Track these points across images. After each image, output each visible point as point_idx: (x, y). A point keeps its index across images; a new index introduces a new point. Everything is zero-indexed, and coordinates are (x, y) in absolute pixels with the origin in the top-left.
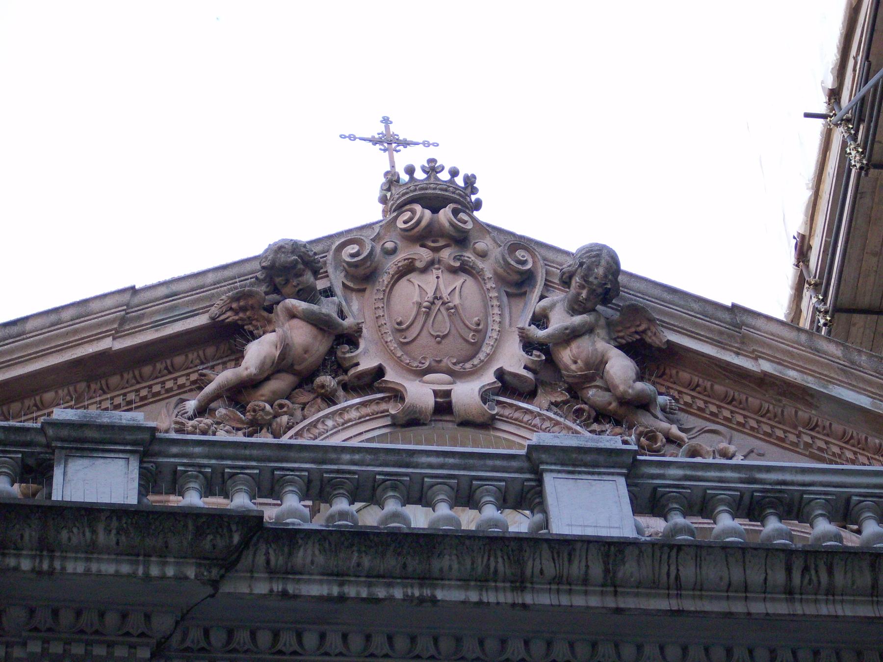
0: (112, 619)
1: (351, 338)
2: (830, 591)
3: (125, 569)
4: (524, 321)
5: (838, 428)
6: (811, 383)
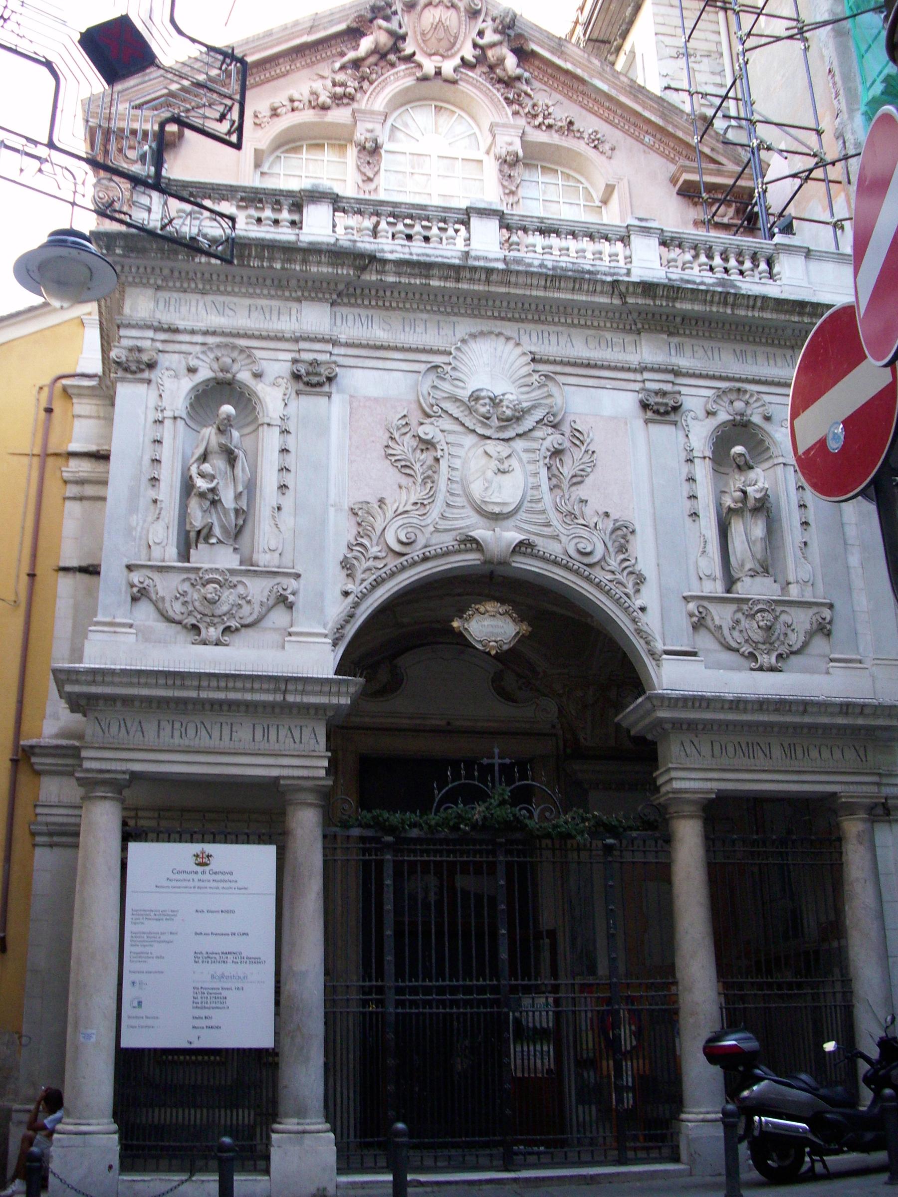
0: (325, 285)
1: (403, 38)
2: (559, 288)
3: (330, 270)
4: (474, 34)
5: (593, 96)
6: (586, 77)
